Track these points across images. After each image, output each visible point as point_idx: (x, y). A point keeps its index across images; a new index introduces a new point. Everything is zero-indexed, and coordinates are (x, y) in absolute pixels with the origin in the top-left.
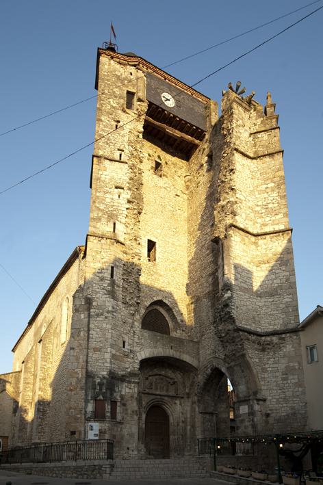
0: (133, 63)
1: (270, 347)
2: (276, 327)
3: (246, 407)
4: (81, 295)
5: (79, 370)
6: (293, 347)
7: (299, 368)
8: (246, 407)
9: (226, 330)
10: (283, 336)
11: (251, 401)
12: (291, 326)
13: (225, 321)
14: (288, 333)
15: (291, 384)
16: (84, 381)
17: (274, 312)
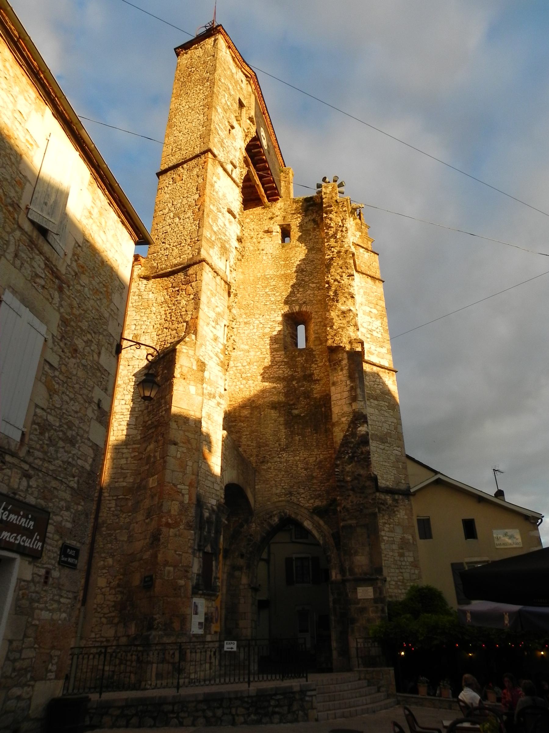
0: (247, 73)
1: (383, 507)
2: (388, 483)
3: (370, 590)
4: (191, 352)
5: (184, 488)
6: (406, 514)
7: (413, 544)
8: (370, 590)
9: (356, 473)
10: (396, 497)
11: (379, 582)
12: (403, 487)
13: (359, 461)
14: (401, 494)
15: (408, 564)
16: (192, 511)
17: (386, 464)
